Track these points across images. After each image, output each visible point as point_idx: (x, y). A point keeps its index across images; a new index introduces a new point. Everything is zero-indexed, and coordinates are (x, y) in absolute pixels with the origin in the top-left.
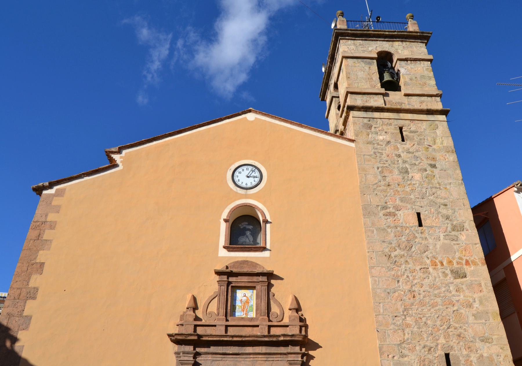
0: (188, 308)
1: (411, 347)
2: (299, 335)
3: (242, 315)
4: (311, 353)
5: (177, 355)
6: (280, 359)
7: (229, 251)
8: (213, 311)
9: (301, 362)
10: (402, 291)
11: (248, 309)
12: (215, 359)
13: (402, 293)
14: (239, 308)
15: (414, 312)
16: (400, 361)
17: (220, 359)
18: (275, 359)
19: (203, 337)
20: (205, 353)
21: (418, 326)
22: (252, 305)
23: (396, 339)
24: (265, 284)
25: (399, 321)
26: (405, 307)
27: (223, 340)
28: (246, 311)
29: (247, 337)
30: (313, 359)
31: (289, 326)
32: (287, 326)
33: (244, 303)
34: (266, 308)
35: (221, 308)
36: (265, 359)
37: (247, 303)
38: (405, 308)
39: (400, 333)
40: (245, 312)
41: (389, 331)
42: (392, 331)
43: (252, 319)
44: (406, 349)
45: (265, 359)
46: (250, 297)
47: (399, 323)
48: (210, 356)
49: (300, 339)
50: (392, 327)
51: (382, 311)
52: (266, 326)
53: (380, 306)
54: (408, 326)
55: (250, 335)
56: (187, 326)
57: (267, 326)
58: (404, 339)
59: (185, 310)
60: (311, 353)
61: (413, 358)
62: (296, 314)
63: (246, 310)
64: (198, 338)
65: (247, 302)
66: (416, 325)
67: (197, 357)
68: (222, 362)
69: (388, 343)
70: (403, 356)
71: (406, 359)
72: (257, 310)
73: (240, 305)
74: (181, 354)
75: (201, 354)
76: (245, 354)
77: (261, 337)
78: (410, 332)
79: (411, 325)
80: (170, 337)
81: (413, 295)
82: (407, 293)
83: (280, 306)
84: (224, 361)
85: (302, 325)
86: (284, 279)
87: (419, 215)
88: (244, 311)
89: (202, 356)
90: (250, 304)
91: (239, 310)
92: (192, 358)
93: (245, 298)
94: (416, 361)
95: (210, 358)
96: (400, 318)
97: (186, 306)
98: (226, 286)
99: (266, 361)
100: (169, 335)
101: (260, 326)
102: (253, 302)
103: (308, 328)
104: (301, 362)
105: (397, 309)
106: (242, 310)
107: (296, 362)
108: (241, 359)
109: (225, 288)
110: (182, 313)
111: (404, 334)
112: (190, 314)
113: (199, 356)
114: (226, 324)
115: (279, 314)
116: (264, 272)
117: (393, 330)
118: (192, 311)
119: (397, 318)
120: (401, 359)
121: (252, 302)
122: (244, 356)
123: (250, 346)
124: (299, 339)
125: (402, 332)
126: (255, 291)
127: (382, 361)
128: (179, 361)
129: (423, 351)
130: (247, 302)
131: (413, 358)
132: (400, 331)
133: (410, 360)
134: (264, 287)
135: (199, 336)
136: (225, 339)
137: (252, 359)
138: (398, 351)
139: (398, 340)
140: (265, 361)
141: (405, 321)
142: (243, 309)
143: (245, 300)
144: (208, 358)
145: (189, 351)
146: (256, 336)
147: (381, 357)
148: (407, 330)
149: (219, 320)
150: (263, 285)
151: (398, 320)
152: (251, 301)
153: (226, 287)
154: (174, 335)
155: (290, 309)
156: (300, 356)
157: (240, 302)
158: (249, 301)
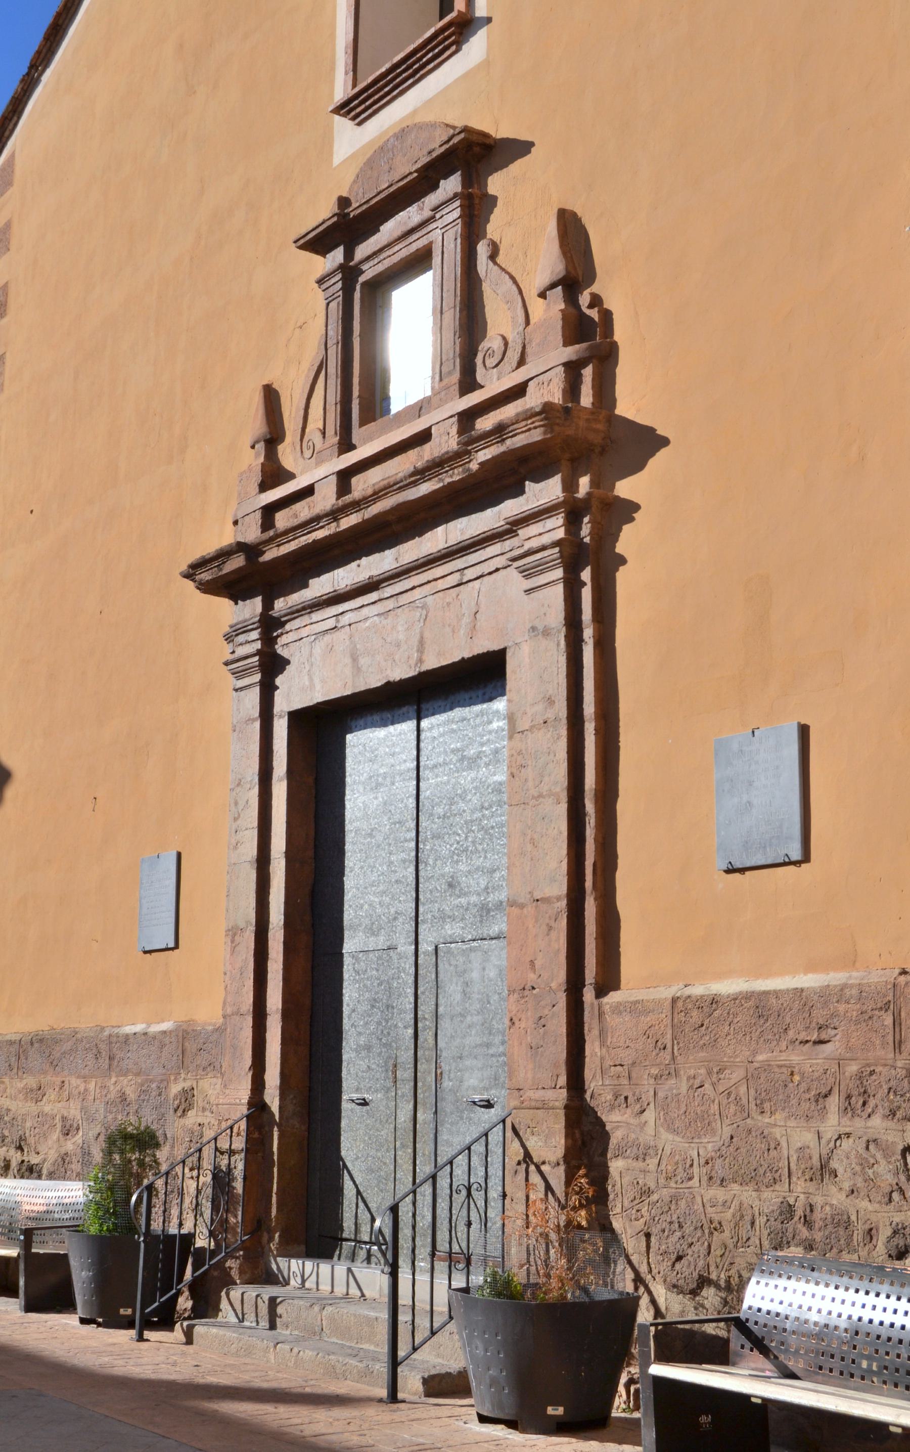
2: (526, 419)
4: (625, 489)
7: (360, 119)
9: (557, 550)
19: (264, 552)
20: (293, 613)
29: (375, 501)
30: (633, 519)
49: (536, 436)
55: (377, 487)
60: (625, 489)
64: (248, 559)
67: (275, 634)
75: (283, 619)
77: (414, 484)
85: (574, 358)
86: (532, 144)
89: (288, 627)
103: (616, 363)
104: (557, 550)
113: (280, 631)
116: (434, 155)
123: (414, 538)
124: (531, 441)
136: (320, 534)
146: (395, 484)
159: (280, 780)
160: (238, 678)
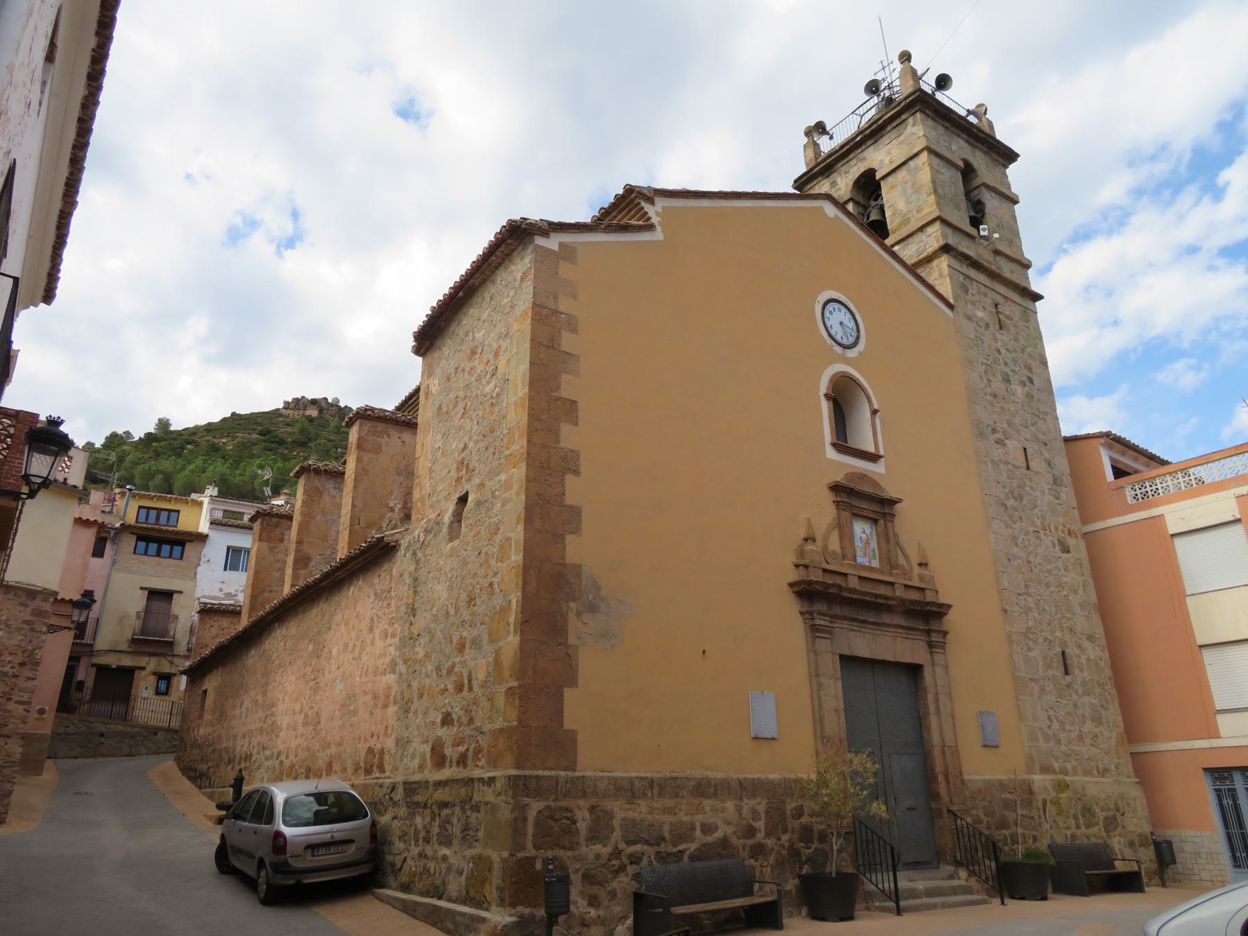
12: (852, 628)
17: (857, 629)
18: (910, 637)
36: (904, 636)
45: (904, 636)
54: (1030, 609)
87: (1025, 449)
95: (846, 626)
97: (802, 536)
108: (879, 632)
129: (1045, 644)
136: (868, 599)
137: (892, 634)
148: (1030, 614)
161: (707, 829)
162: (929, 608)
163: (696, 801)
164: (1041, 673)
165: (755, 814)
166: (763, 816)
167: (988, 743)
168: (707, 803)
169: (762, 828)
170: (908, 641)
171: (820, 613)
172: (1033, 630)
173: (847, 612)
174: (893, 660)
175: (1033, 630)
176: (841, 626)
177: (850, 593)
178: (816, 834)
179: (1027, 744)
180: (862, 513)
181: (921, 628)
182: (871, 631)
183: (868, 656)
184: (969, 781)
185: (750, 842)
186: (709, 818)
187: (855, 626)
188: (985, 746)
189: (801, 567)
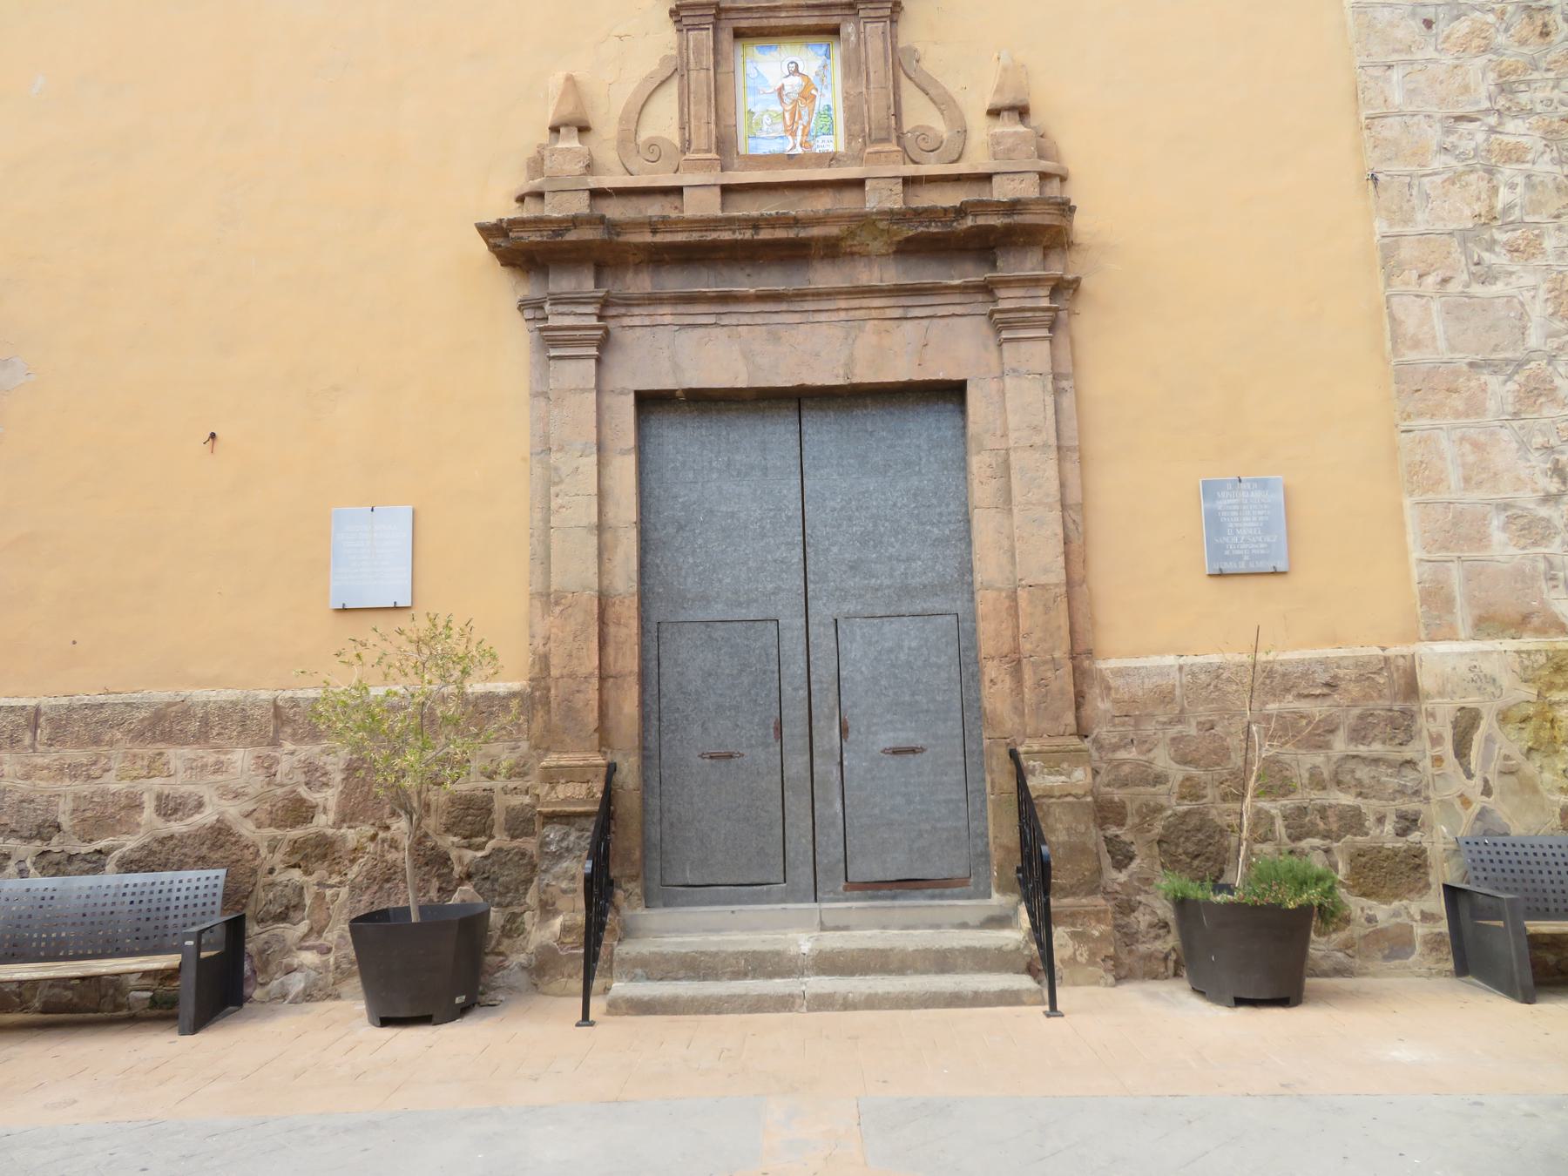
0: (555, 130)
1: (1520, 241)
3: (788, 148)
5: (529, 314)
6: (958, 310)
8: (666, 136)
10: (1492, 10)
11: (812, 125)
13: (1491, 18)
14: (773, 123)
15: (1540, 95)
16: (1470, 297)
17: (712, 320)
21: (1555, 154)
22: (829, 109)
23: (1460, 210)
24: (880, 13)
25: (1473, 137)
26: (1500, 77)
27: (713, 241)
28: (806, 133)
31: (995, 179)
32: (987, 178)
33: (795, 102)
34: (889, 108)
35: (698, 119)
36: (898, 313)
37: (806, 99)
38: (1501, 81)
39: (1477, 182)
40: (799, 138)
41: (1425, 180)
42: (1438, 179)
43: (832, 159)
44: (1497, 249)
45: (898, 313)
46: (817, 74)
47: (1473, 144)
48: (667, 309)
50: (1438, 162)
51: (1397, 98)
52: (894, 181)
53: (1388, 80)
54: (1514, 154)
56: (559, 196)
57: (901, 180)
58: (1492, 208)
59: (545, 136)
61: (1529, 280)
62: (1021, 128)
63: (805, 127)
65: (807, 96)
66: (1548, 150)
68: (718, 330)
69: (1422, 228)
70: (1488, 277)
71: (1498, 288)
72: (849, 122)
73: (779, 108)
74: (547, 307)
76: (813, 295)
78: (1520, 180)
79: (1527, 150)
80: (491, 240)
81: (1539, 23)
82: (1510, 18)
83: (943, 103)
84: (725, 329)
88: (794, 134)
90: (817, 103)
91: (774, 131)
92: (595, 318)
93: (796, 80)
94: (1542, 295)
95: (668, 319)
96: (1478, 123)
97: (549, 120)
98: (711, 26)
99: (904, 322)
100: (487, 231)
101: (868, 183)
102: (831, 96)
105: (1466, 89)
106: (786, 131)
107: (1029, 314)
108: (796, 318)
109: (708, 36)
110: (532, 152)
111: (1495, 190)
112: (569, 150)
114: (725, 182)
115: (945, 136)
117: (1445, 176)
118: (577, 139)
119: (1464, 127)
120: (1477, 289)
121: (828, 94)
122: (811, 303)
125: (1486, 182)
126: (837, 52)
127: (1394, 300)
128: (541, 330)
130: (807, 96)
131: (1529, 280)
132: (1473, 177)
133: (1515, 292)
134: (876, 25)
135: (613, 226)
136: (726, 236)
137: (843, 315)
138: (1463, 258)
139: (1467, 212)
140: (897, 322)
141: (1498, 136)
142: (788, 123)
143: (798, 90)
144: (659, 320)
145: (578, 293)
147: (1388, 285)
148: (1508, 171)
149: (696, 165)
150: (873, 14)
151: (1469, 134)
152: (824, 91)
153: (711, 32)
154: (505, 225)
155: (994, 113)
156: (1046, 292)
157: (775, 97)
158: (813, 92)
159: (624, 453)
160: (553, 347)
161: (169, 807)
162: (969, 222)
163: (151, 750)
164: (1534, 340)
165: (314, 774)
166: (338, 777)
167: (1228, 567)
168: (176, 756)
169: (332, 803)
170: (908, 325)
171: (557, 301)
172: (1516, 214)
173: (674, 282)
174: (840, 381)
175: (1516, 214)
176: (647, 321)
177: (654, 232)
178: (499, 816)
179: (1416, 554)
180: (773, 22)
181: (957, 282)
182: (759, 319)
183: (742, 383)
184: (1120, 673)
185: (297, 833)
186: (180, 785)
187: (701, 314)
188: (1221, 575)
189: (527, 199)
